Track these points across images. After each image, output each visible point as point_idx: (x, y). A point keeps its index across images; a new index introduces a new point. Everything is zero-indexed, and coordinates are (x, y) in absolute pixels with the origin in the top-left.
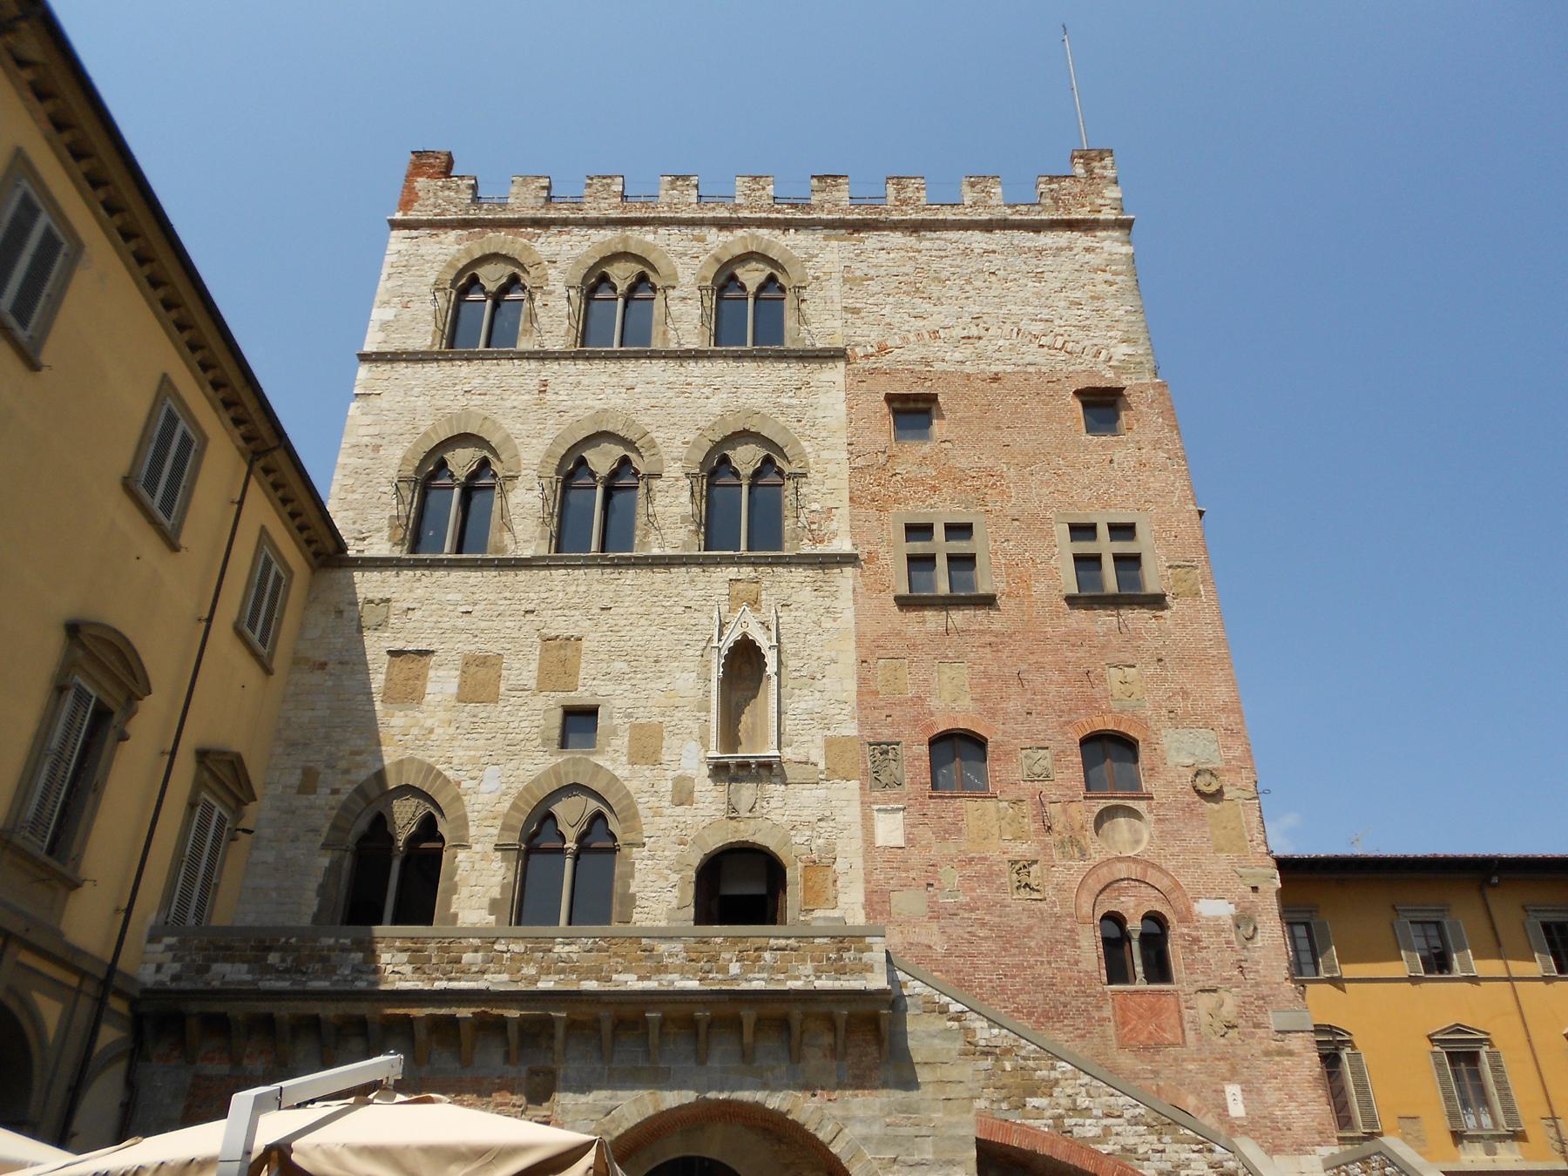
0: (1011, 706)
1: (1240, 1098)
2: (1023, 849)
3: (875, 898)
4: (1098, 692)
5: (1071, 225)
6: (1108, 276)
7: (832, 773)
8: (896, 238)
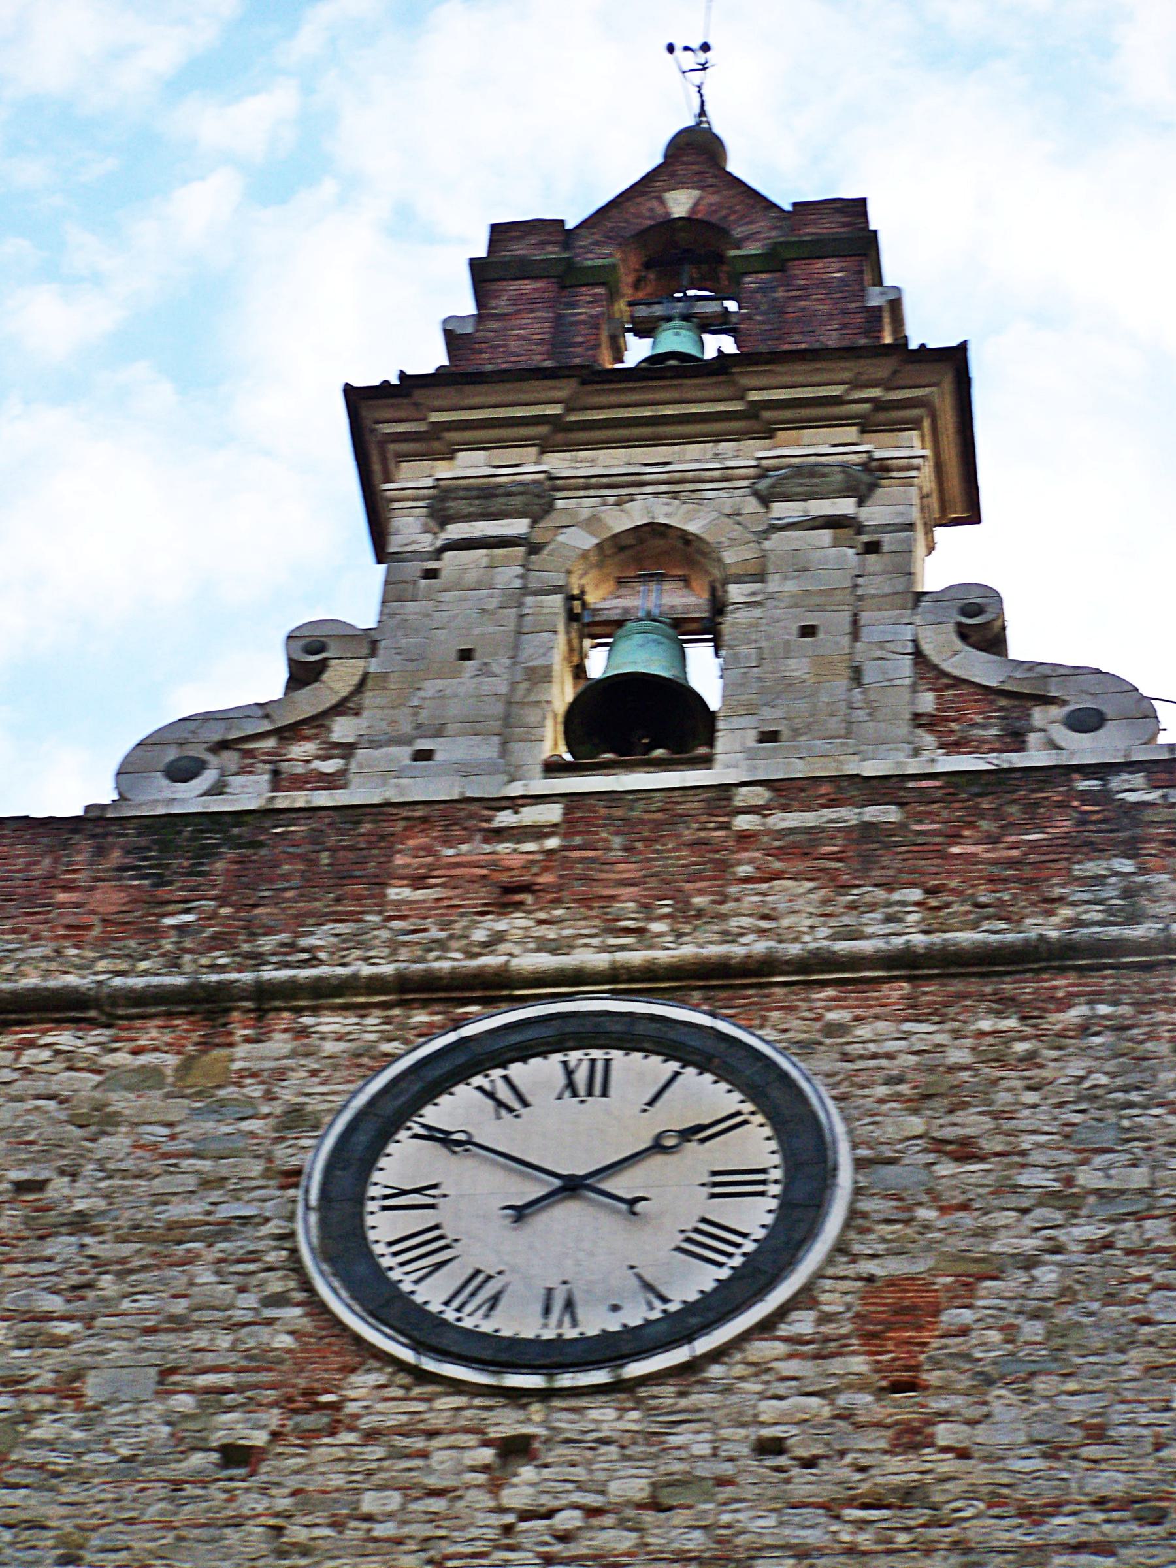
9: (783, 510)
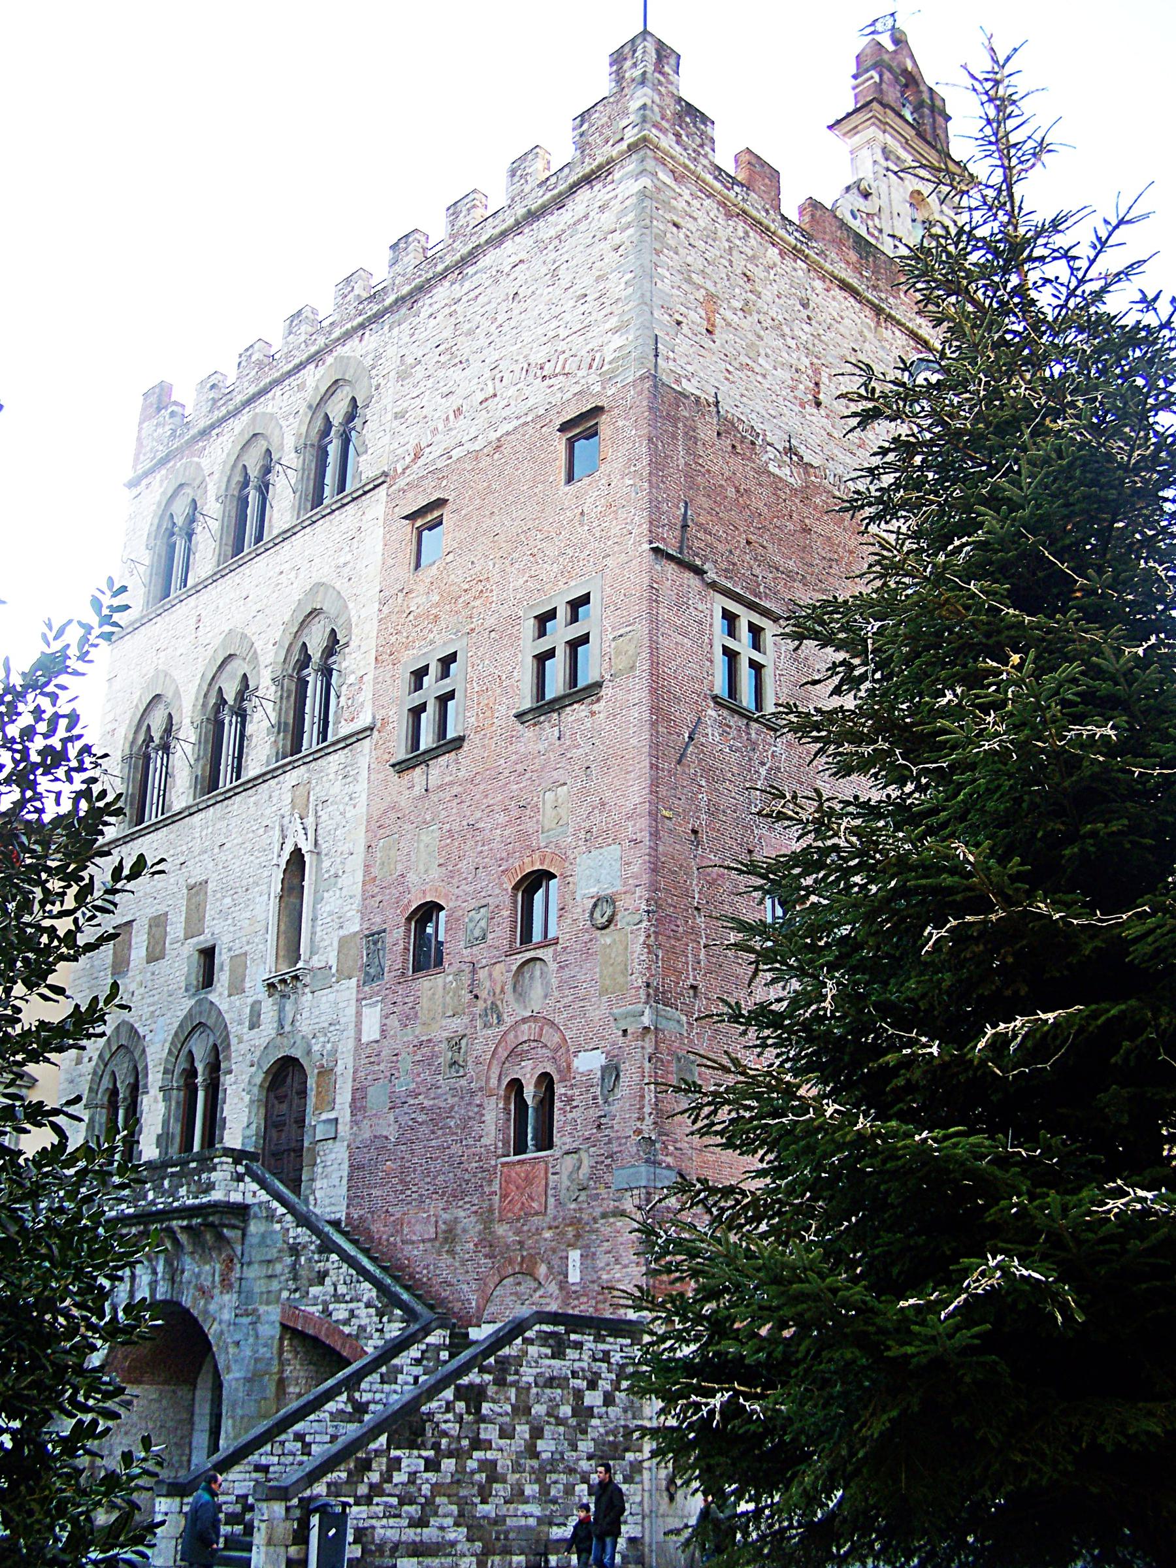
0: (462, 865)
1: (578, 1264)
2: (457, 1024)
3: (358, 1095)
4: (530, 826)
6: (617, 238)
7: (344, 975)
8: (442, 292)
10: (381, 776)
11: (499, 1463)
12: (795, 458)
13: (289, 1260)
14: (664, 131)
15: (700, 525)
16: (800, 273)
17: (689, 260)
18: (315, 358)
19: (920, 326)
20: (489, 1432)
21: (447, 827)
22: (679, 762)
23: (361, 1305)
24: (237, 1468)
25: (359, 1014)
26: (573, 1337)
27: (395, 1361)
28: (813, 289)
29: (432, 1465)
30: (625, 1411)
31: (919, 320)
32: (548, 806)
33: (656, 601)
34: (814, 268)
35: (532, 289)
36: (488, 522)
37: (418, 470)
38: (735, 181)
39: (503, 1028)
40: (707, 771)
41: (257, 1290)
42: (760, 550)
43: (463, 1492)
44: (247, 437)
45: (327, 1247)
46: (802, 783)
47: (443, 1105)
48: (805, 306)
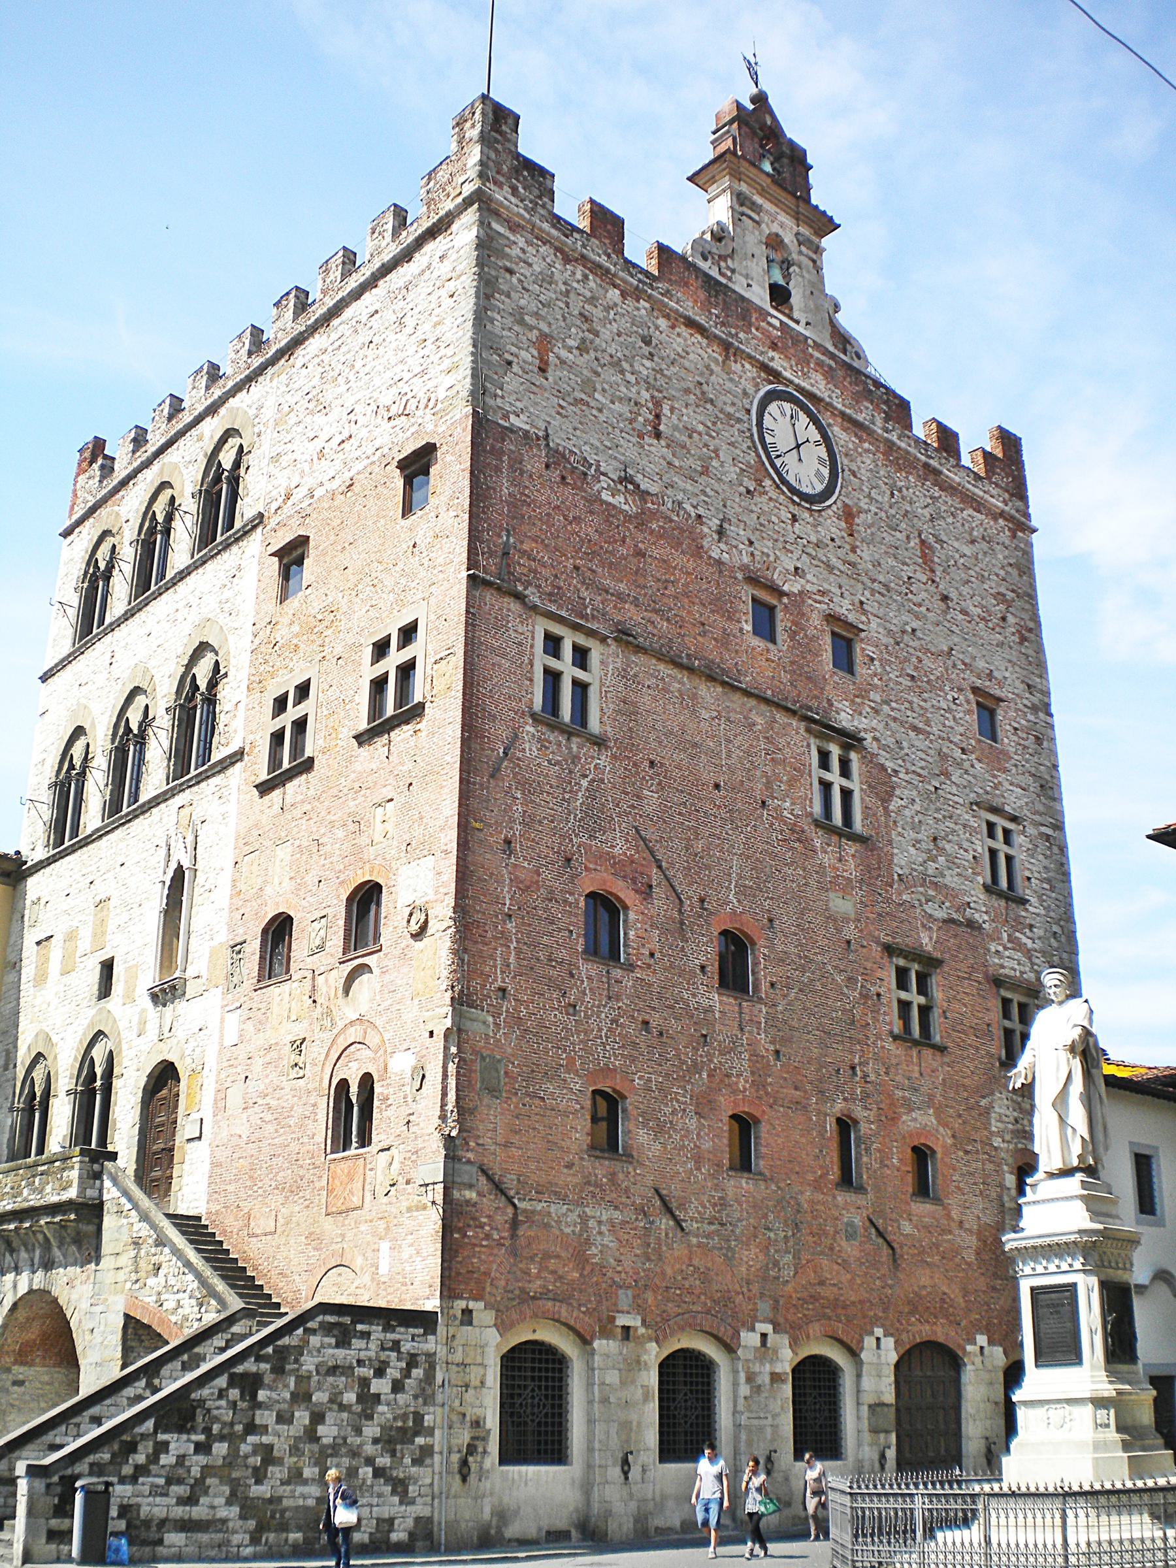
2: (299, 1030)
5: (432, 233)
8: (315, 343)
9: (803, 248)
10: (248, 797)
11: (276, 1447)
12: (630, 487)
13: (133, 1253)
14: (500, 185)
15: (524, 553)
16: (643, 312)
17: (523, 302)
18: (212, 410)
19: (772, 359)
20: (266, 1417)
21: (297, 843)
22: (492, 776)
23: (186, 1295)
24: (30, 1447)
25: (222, 1020)
26: (359, 1327)
27: (196, 1350)
28: (657, 328)
29: (202, 1448)
30: (416, 1397)
31: (771, 354)
32: (379, 819)
33: (474, 625)
34: (657, 307)
35: (384, 336)
36: (341, 556)
37: (287, 509)
38: (574, 229)
39: (335, 1031)
40: (523, 784)
41: (108, 1281)
42: (588, 574)
43: (234, 1475)
44: (156, 484)
45: (160, 1242)
46: (627, 794)
47: (285, 1105)
48: (647, 341)
